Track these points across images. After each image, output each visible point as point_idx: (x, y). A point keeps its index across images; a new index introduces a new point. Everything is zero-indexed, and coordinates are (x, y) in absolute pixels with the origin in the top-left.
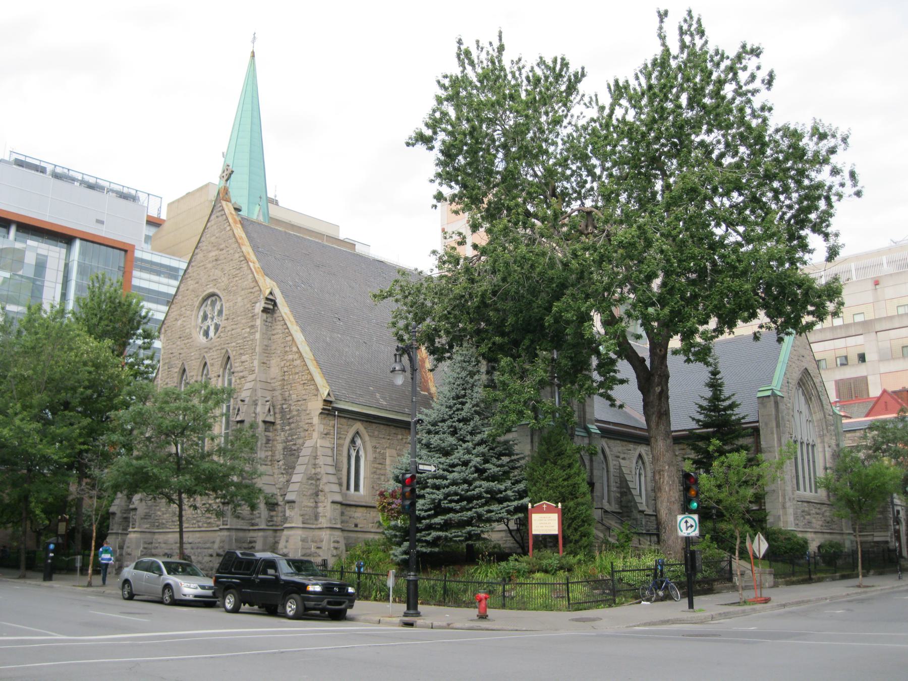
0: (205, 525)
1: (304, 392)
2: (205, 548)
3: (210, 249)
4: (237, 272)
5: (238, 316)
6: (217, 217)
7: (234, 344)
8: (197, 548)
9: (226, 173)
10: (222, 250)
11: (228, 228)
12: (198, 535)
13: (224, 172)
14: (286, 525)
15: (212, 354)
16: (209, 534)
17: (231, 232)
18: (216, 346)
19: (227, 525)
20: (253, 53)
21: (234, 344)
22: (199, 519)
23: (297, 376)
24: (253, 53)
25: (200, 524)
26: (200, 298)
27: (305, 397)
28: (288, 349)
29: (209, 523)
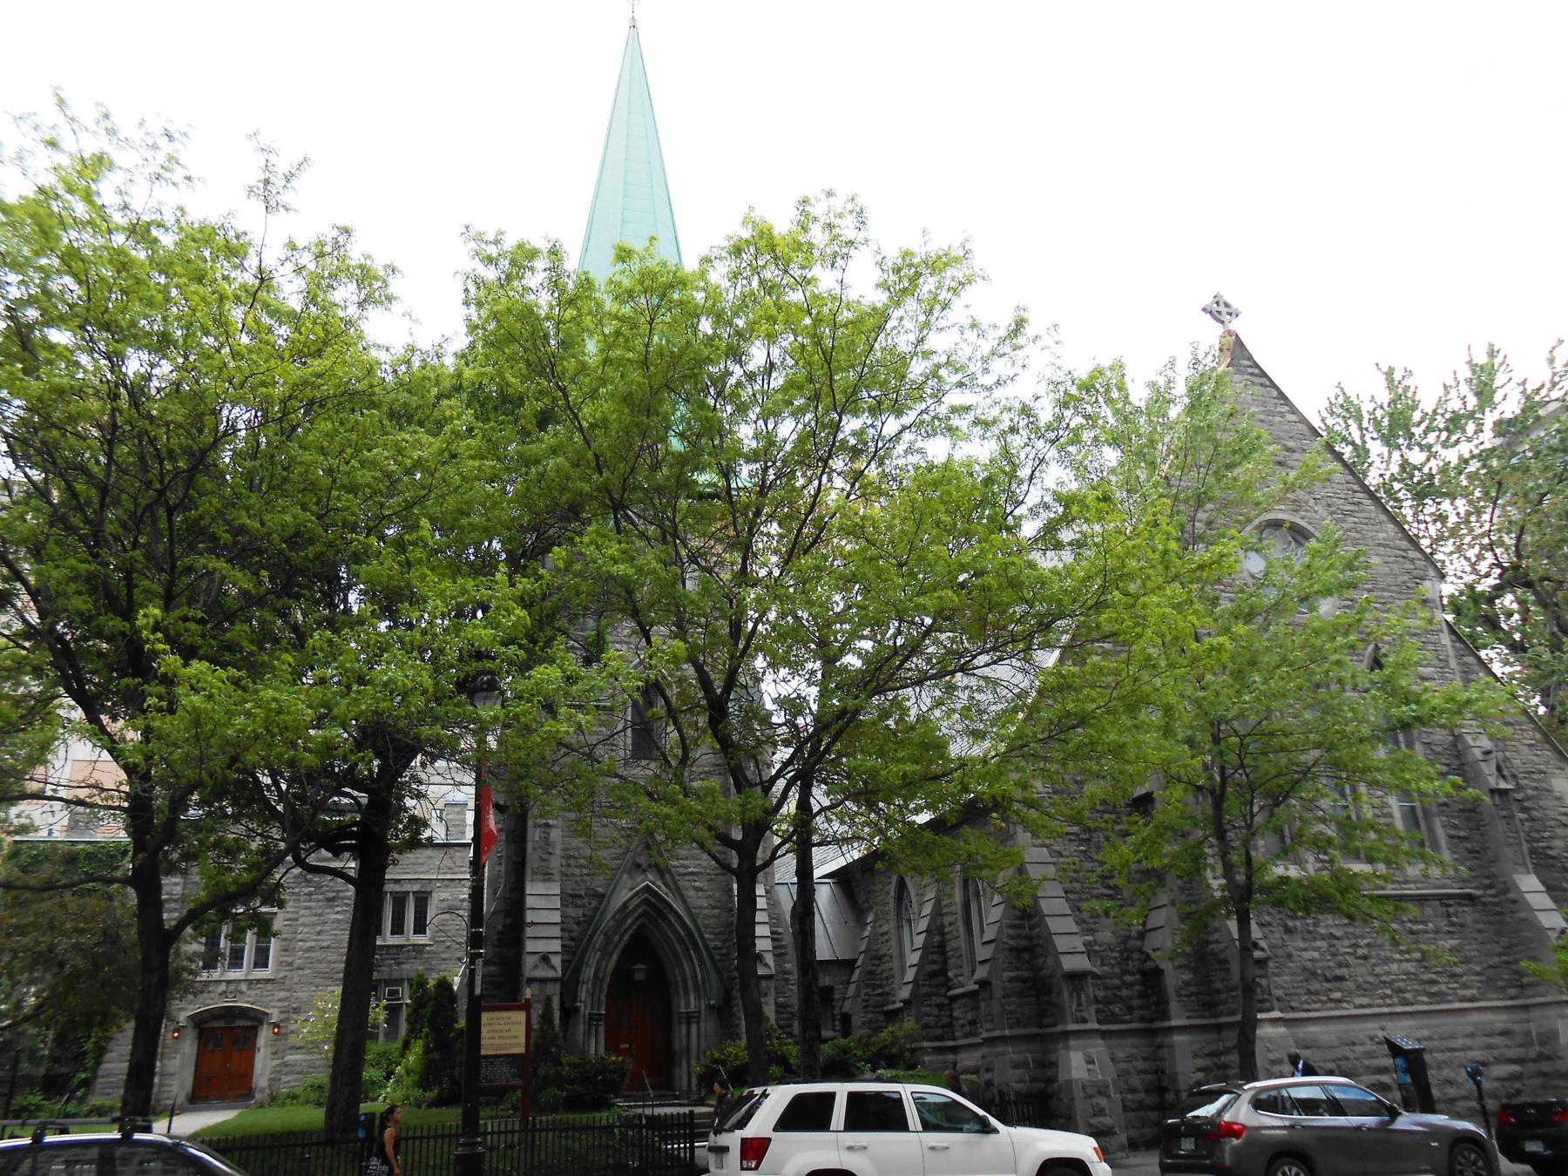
0: (1425, 999)
1: (1535, 758)
5: (1382, 590)
9: (1222, 308)
10: (1288, 449)
11: (1293, 418)
13: (1227, 305)
27: (1543, 768)
29: (1434, 994)
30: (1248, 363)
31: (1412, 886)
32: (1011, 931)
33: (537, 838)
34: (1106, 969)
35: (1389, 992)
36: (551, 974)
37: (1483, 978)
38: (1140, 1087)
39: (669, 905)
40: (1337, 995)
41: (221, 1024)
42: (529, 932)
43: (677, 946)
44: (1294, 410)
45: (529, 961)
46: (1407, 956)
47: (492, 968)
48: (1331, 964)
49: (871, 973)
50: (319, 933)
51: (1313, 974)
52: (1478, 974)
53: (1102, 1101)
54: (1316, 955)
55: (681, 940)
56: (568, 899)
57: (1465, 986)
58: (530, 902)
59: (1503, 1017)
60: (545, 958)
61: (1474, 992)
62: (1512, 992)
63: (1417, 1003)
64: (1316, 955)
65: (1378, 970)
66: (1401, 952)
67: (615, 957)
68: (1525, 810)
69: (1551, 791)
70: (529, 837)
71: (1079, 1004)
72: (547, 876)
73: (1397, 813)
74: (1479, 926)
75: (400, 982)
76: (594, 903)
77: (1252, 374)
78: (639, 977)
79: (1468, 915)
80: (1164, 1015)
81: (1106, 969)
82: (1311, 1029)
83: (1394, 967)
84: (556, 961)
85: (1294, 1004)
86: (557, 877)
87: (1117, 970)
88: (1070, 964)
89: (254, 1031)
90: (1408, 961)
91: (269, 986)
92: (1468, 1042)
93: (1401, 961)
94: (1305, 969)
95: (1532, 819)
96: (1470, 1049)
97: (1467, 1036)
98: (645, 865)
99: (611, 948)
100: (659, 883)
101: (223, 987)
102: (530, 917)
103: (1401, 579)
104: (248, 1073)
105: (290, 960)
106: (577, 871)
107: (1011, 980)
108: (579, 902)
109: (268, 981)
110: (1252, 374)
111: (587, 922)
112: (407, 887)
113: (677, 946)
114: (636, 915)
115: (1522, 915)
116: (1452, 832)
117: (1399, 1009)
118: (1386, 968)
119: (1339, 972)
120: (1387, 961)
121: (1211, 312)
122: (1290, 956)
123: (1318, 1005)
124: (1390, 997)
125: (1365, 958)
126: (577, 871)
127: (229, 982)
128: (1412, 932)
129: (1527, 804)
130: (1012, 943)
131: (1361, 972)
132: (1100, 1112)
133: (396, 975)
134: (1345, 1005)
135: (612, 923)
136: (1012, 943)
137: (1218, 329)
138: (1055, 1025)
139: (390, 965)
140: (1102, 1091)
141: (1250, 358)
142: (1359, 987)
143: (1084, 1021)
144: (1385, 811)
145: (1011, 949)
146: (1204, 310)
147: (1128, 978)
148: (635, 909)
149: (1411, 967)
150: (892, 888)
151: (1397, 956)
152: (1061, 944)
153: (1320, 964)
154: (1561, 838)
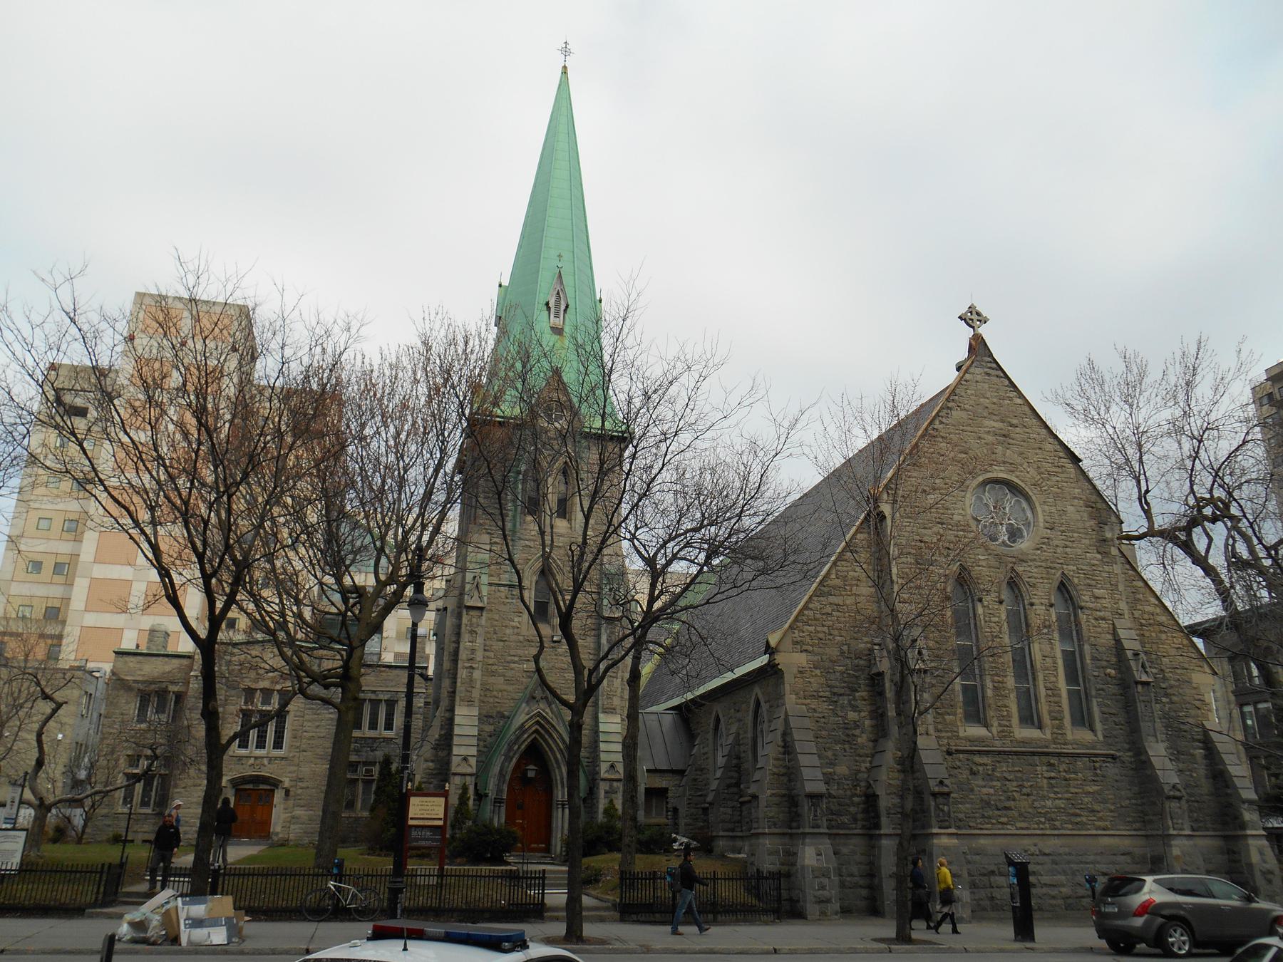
0: (1070, 826)
2: (1087, 863)
3: (985, 414)
4: (1057, 469)
5: (1073, 531)
6: (988, 374)
7: (1071, 567)
8: (1069, 863)
9: (975, 317)
11: (1019, 401)
12: (1056, 841)
13: (978, 314)
14: (1249, 832)
15: (1029, 569)
16: (1082, 840)
17: (1027, 409)
18: (1035, 560)
19: (1181, 829)
20: (565, 67)
21: (1071, 567)
22: (1053, 816)
23: (1164, 636)
24: (565, 67)
25: (1057, 823)
26: (981, 479)
27: (1186, 665)
28: (1141, 596)
30: (989, 359)
31: (1070, 747)
32: (775, 762)
33: (464, 676)
34: (841, 792)
35: (1043, 820)
36: (469, 770)
37: (1116, 815)
38: (857, 874)
39: (553, 726)
40: (1004, 820)
41: (250, 786)
42: (456, 740)
43: (559, 756)
44: (1021, 395)
45: (455, 760)
46: (1060, 796)
47: (431, 764)
48: (1002, 798)
49: (695, 780)
50: (318, 727)
51: (988, 803)
52: (1111, 811)
53: (826, 881)
54: (992, 791)
55: (560, 750)
56: (484, 718)
57: (1100, 819)
58: (457, 720)
59: (1127, 842)
60: (465, 759)
61: (1108, 823)
62: (1138, 825)
63: (1063, 828)
64: (992, 791)
65: (1036, 804)
66: (1056, 793)
67: (514, 760)
68: (1166, 695)
69: (1189, 682)
70: (459, 676)
71: (815, 816)
72: (470, 702)
73: (1064, 694)
74: (1117, 778)
75: (373, 764)
76: (502, 723)
77: (990, 368)
78: (531, 774)
79: (1112, 770)
80: (877, 826)
81: (841, 792)
82: (982, 841)
83: (1049, 803)
84: (473, 761)
85: (971, 824)
86: (477, 704)
87: (849, 793)
88: (810, 787)
89: (271, 793)
90: (1060, 799)
91: (283, 763)
92: (1099, 858)
93: (1055, 799)
94: (982, 800)
95: (1172, 702)
96: (1098, 863)
97: (1096, 854)
98: (538, 698)
99: (511, 754)
100: (548, 710)
101: (252, 761)
102: (457, 731)
103: (1088, 524)
104: (266, 823)
105: (298, 744)
106: (491, 700)
107: (773, 795)
108: (491, 720)
109: (282, 758)
110: (990, 368)
111: (497, 734)
112: (381, 697)
113: (559, 756)
114: (531, 731)
115: (1149, 772)
116: (1105, 709)
117: (1048, 832)
118: (1043, 803)
119: (1007, 804)
120: (1044, 798)
121: (965, 320)
122: (972, 790)
123: (989, 826)
124: (1044, 823)
125: (1028, 795)
126: (491, 700)
127: (256, 758)
128: (1066, 780)
129: (1169, 691)
130: (775, 770)
131: (1024, 804)
132: (823, 888)
133: (371, 759)
134: (1009, 827)
135: (513, 737)
136: (775, 770)
137: (970, 332)
138: (798, 828)
139: (367, 752)
140: (825, 874)
141: (991, 355)
142: (1021, 815)
143: (818, 827)
144: (1055, 692)
145: (774, 774)
146: (960, 317)
147: (856, 799)
148: (530, 727)
149: (1061, 803)
150: (712, 721)
151: (1052, 795)
152: (806, 773)
153: (993, 798)
154: (1193, 717)
